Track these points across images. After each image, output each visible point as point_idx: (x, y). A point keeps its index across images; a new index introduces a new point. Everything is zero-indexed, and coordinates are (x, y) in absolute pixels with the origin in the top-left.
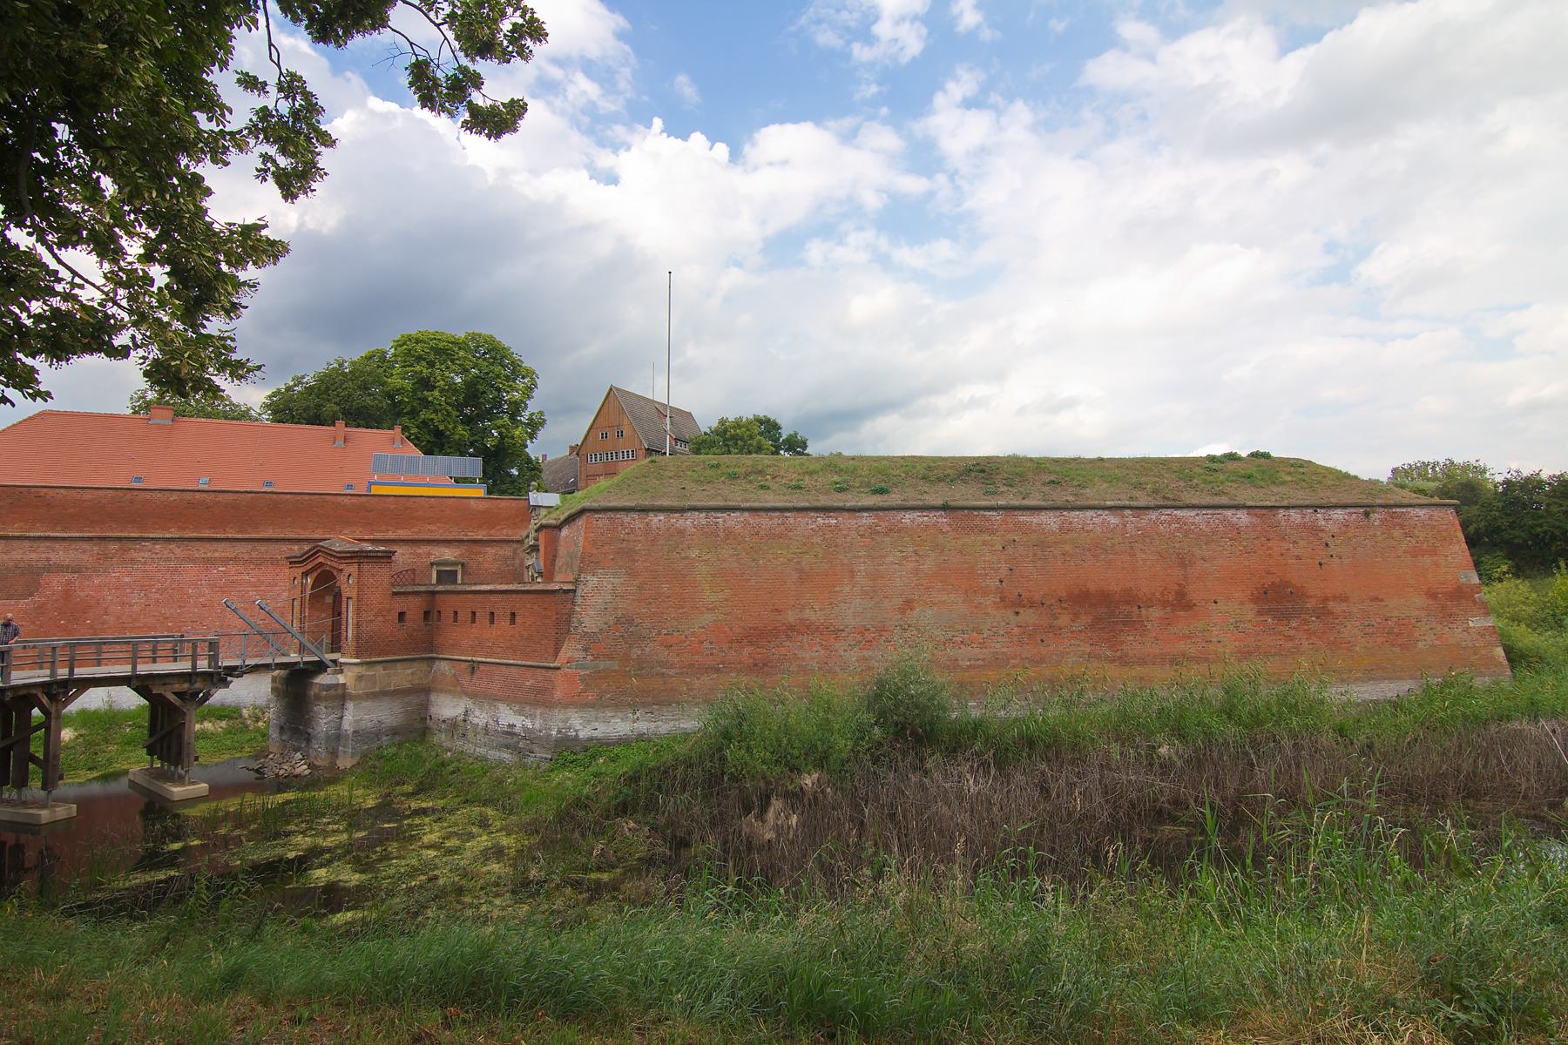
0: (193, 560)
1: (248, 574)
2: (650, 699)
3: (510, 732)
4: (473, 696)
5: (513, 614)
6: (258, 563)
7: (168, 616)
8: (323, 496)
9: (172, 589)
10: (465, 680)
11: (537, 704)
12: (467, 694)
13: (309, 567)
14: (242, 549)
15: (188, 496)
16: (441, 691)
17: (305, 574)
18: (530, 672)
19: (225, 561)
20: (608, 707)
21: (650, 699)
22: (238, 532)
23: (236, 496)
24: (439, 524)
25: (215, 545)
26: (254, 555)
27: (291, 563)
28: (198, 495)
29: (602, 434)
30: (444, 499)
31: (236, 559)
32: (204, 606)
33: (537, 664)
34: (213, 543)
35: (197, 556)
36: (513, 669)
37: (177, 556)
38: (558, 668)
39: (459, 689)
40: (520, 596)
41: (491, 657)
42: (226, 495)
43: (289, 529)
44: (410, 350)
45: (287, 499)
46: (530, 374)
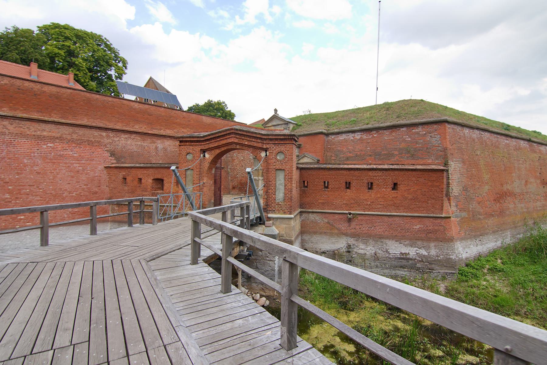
0: (22, 135)
1: (72, 150)
2: (479, 233)
3: (404, 257)
4: (354, 236)
5: (395, 184)
6: (79, 143)
7: (7, 180)
9: (9, 159)
10: (343, 226)
11: (430, 240)
12: (346, 235)
14: (65, 131)
15: (18, 83)
16: (315, 233)
17: (204, 151)
19: (53, 139)
20: (468, 239)
21: (479, 233)
22: (62, 118)
23: (58, 89)
25: (43, 126)
26: (75, 136)
27: (181, 142)
28: (27, 84)
29: (145, 99)
31: (61, 139)
32: (38, 173)
33: (426, 215)
34: (41, 124)
35: (28, 133)
36: (397, 219)
37: (10, 131)
38: (450, 217)
39: (336, 231)
40: (403, 173)
41: (369, 210)
42: (51, 87)
43: (99, 120)
44: (61, 32)
45: (97, 99)
46: (125, 63)
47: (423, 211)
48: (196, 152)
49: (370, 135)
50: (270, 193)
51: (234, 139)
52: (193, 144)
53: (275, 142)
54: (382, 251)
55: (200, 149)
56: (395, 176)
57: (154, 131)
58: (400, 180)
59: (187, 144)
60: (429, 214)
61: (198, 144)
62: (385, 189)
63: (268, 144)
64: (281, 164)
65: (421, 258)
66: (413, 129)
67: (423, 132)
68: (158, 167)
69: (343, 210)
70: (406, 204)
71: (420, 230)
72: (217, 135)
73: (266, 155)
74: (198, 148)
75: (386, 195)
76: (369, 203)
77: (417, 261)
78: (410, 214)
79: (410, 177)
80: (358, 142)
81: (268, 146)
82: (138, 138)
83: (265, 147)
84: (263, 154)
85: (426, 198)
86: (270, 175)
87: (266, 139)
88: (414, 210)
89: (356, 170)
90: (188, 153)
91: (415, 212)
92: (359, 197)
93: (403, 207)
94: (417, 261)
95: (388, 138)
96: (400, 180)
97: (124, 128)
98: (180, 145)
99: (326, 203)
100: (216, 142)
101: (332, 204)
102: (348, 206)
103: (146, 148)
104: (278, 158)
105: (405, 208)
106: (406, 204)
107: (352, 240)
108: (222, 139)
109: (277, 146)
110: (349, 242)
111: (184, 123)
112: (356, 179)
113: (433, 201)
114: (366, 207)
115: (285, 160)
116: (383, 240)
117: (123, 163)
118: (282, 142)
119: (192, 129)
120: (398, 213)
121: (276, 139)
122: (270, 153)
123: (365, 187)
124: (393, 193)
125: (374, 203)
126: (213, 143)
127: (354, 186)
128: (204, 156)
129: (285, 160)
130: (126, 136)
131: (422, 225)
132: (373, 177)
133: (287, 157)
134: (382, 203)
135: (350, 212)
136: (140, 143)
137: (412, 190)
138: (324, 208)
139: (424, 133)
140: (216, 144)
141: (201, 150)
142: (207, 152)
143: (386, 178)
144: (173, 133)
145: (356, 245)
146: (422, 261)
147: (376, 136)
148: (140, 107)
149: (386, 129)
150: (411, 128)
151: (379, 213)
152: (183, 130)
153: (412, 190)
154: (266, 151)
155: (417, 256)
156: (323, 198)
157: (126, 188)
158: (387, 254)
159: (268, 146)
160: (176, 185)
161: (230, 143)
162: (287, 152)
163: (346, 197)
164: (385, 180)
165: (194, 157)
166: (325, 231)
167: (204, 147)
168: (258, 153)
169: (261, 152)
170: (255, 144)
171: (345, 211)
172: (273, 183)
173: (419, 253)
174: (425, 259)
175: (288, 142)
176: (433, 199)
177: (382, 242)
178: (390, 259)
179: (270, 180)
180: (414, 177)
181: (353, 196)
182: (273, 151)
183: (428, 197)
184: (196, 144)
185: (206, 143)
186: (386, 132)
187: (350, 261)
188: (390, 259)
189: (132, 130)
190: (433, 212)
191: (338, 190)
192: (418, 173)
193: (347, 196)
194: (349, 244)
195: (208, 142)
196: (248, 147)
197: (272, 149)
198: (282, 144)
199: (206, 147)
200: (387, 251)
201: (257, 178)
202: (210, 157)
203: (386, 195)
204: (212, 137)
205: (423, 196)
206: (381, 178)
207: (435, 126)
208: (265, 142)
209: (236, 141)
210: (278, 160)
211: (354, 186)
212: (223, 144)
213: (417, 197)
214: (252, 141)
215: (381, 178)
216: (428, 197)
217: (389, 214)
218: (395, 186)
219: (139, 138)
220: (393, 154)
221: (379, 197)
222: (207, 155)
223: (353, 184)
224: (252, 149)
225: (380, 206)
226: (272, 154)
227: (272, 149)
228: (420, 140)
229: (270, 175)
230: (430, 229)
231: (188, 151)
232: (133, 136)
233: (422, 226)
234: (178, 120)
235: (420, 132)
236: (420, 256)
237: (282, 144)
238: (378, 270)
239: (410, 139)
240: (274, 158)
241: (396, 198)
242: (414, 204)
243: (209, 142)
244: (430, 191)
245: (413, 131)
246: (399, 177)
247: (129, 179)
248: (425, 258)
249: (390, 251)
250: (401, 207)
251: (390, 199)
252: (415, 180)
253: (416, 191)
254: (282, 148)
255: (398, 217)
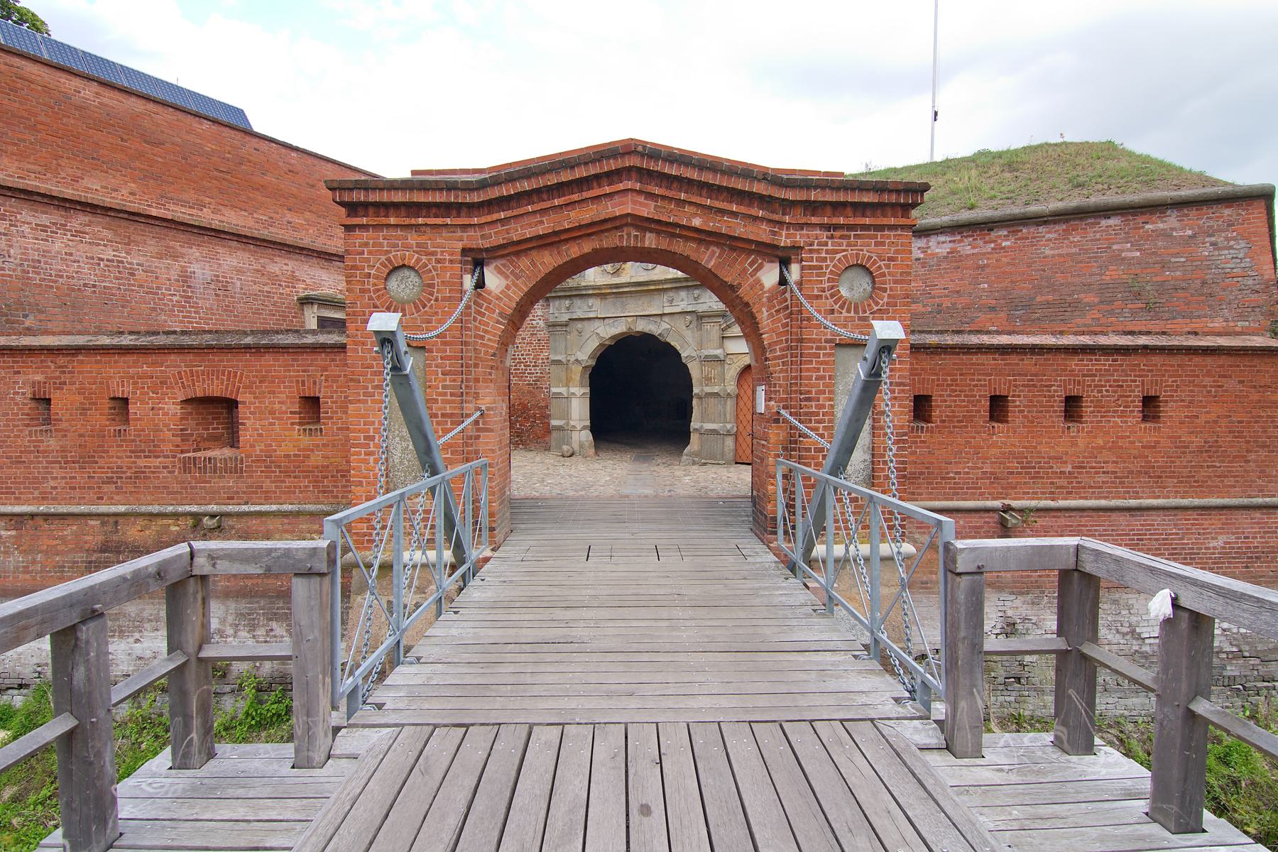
8: (16, 61)
13: (521, 231)
17: (477, 260)
18: (1216, 520)
24: (307, 215)
30: (316, 161)
33: (1246, 501)
36: (1157, 519)
40: (1175, 361)
41: (1069, 495)
47: (1234, 486)
48: (438, 261)
49: (985, 243)
50: (809, 450)
51: (634, 202)
52: (420, 221)
53: (835, 221)
54: (1118, 632)
55: (460, 245)
56: (1152, 371)
57: (172, 207)
58: (1166, 386)
59: (392, 221)
60: (1250, 496)
61: (448, 221)
62: (1119, 417)
63: (801, 226)
64: (860, 319)
65: (1236, 645)
66: (1147, 223)
67: (1183, 229)
68: (211, 347)
69: (982, 496)
70: (1185, 467)
71: (1226, 553)
72: (552, 179)
73: (783, 281)
74: (450, 244)
75: (1122, 437)
76: (1069, 468)
77: (1224, 656)
78: (1197, 502)
79: (1198, 376)
80: (944, 265)
81: (800, 238)
82: (99, 228)
83: (784, 240)
84: (769, 276)
85: (1244, 446)
86: (809, 370)
87: (794, 204)
88: (1208, 487)
89: (1025, 354)
90: (396, 269)
91: (1211, 493)
92: (1035, 447)
93: (1174, 477)
94: (1224, 656)
95: (1056, 252)
96: (1166, 386)
97: (32, 183)
98: (349, 228)
99: (922, 473)
100: (543, 211)
101: (943, 478)
102: (1000, 482)
103: (140, 274)
104: (844, 292)
105: (1182, 482)
106: (1185, 467)
107: (1019, 602)
108: (575, 197)
109: (842, 237)
110: (1010, 613)
111: (295, 191)
112: (1028, 386)
113: (1263, 453)
114: (1058, 482)
115: (877, 304)
116: (1117, 596)
117: (29, 331)
118: (867, 221)
119: (324, 217)
120: (1158, 497)
121: (837, 207)
122: (810, 268)
123: (1055, 412)
124: (1145, 433)
125: (1084, 468)
126: (526, 220)
127: (1020, 411)
128: (480, 284)
129: (877, 304)
130: (45, 219)
131: (1233, 534)
132: (1084, 375)
133: (885, 290)
134: (1110, 467)
135: (1007, 502)
136: (109, 254)
137: (1203, 418)
138: (913, 493)
139: (1190, 232)
140: (545, 226)
141: (465, 251)
142: (499, 263)
143: (1123, 381)
144: (251, 223)
145: (1034, 619)
146: (1240, 655)
147: (1009, 247)
148: (105, 100)
149: (1045, 223)
150: (1140, 219)
151: (1103, 503)
152: (289, 216)
153: (1203, 418)
154: (785, 263)
155: (1223, 638)
156: (913, 458)
157: (52, 443)
158: (1135, 642)
159: (800, 238)
160: (300, 424)
161: (615, 218)
162: (888, 267)
163: (993, 451)
164: (1122, 386)
165: (432, 286)
166: (925, 578)
167: (483, 237)
168: (745, 270)
169: (760, 267)
170: (740, 229)
171: (987, 499)
172: (823, 406)
173: (1229, 630)
174: (1247, 648)
175: (892, 221)
176: (1263, 446)
177: (1115, 602)
178: (1146, 658)
179: (809, 392)
180: (1209, 374)
181: (1014, 446)
182: (825, 259)
183: (1248, 442)
184: (439, 221)
185: (495, 217)
186: (1048, 233)
187: (1018, 680)
188: (1146, 658)
189: (69, 193)
190: (1262, 492)
191: (966, 427)
192: (1223, 360)
193: (994, 445)
194: (1010, 620)
195: (502, 215)
196: (700, 241)
197: (818, 251)
198: (865, 227)
199: (495, 237)
200: (1133, 632)
201: (562, 390)
202: (508, 287)
203: (1122, 437)
204: (526, 185)
205: (1236, 437)
206: (1108, 381)
207: (1227, 212)
208: (787, 219)
209: (647, 209)
210: (844, 304)
211: (1020, 411)
212: (580, 227)
213: (1217, 441)
214: (722, 212)
215: (1108, 381)
216: (1248, 442)
217: (1133, 503)
218: (1150, 405)
219: (107, 234)
220: (1079, 301)
221: (1102, 448)
222: (493, 280)
223: (1017, 403)
224: (718, 251)
225: (1101, 478)
226: (818, 275)
227: (818, 251)
228: (1177, 255)
229: (809, 370)
230: (1255, 547)
231: (396, 256)
232: (78, 221)
233: (1232, 538)
234: (269, 178)
235: (1172, 229)
236: (1234, 639)
237: (865, 227)
238: (1110, 700)
239: (1138, 254)
240: (828, 293)
241: (1154, 447)
242: (1208, 467)
243: (509, 213)
244: (1256, 422)
245: (1147, 226)
246: (1164, 376)
247: (62, 402)
248: (1248, 643)
249: (1144, 630)
250: (1170, 477)
251: (1136, 452)
252: (1211, 386)
253: (1216, 422)
254: (866, 248)
255: (1161, 513)
